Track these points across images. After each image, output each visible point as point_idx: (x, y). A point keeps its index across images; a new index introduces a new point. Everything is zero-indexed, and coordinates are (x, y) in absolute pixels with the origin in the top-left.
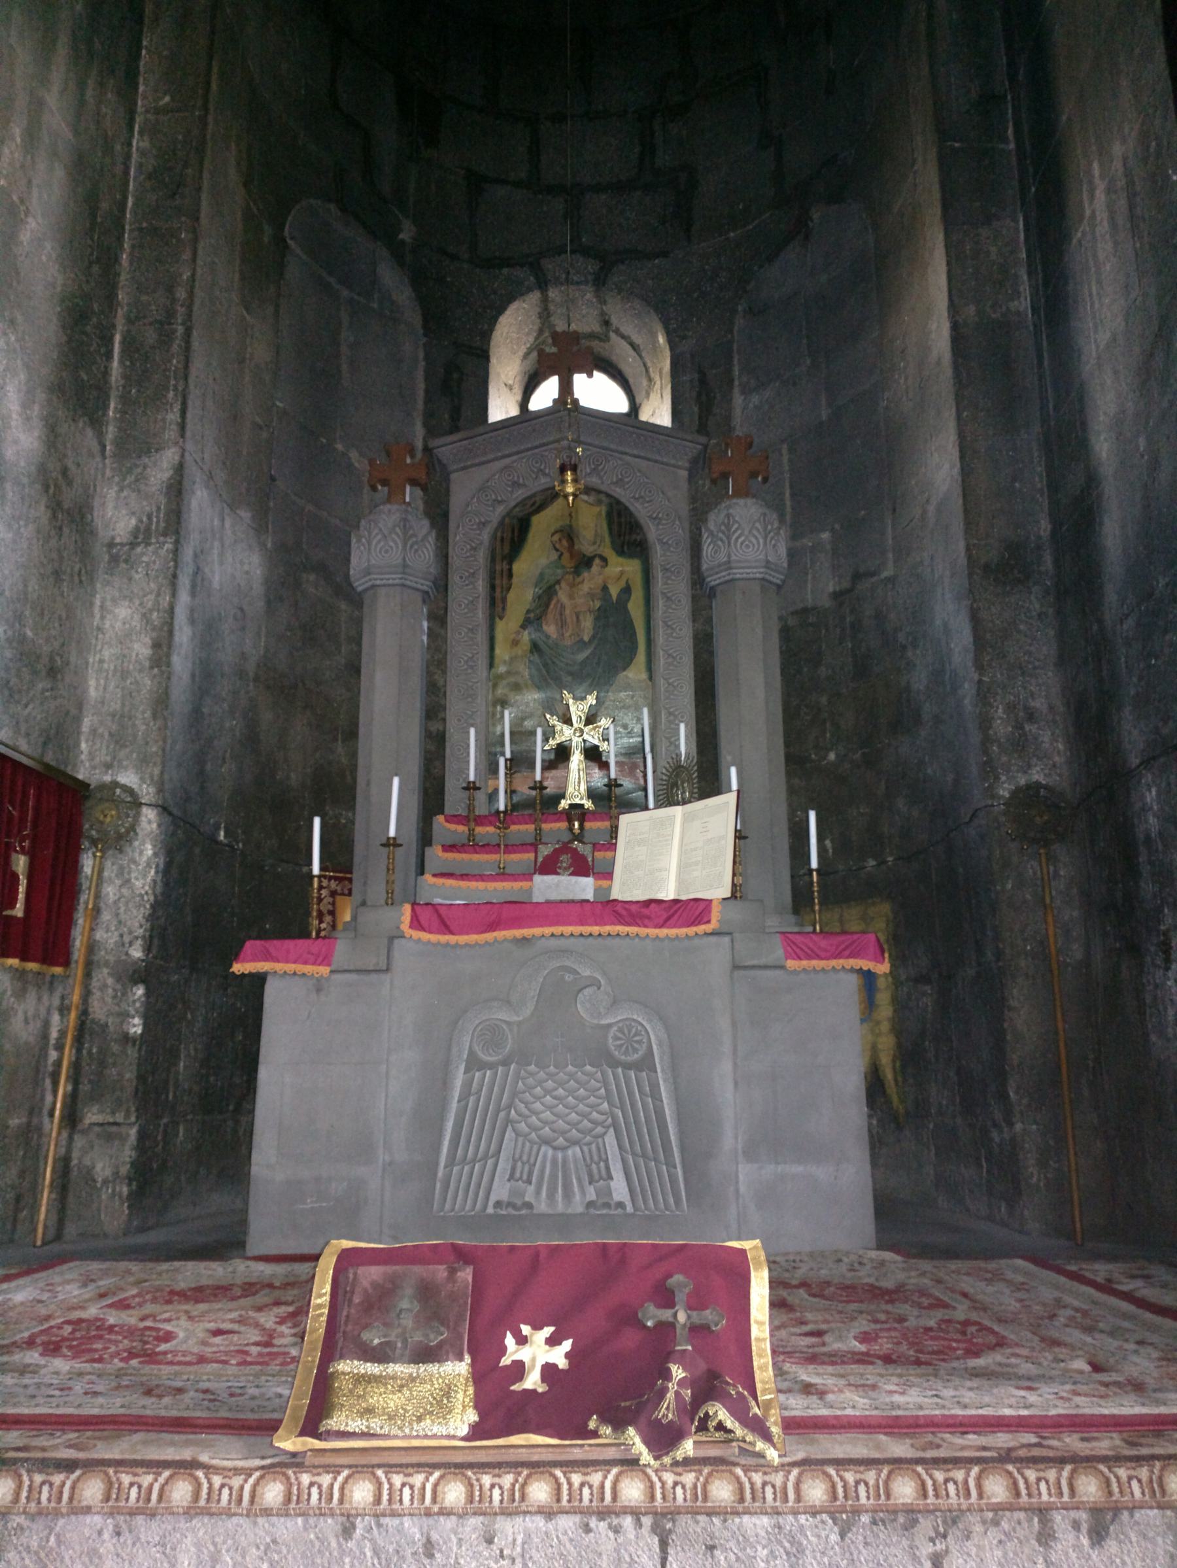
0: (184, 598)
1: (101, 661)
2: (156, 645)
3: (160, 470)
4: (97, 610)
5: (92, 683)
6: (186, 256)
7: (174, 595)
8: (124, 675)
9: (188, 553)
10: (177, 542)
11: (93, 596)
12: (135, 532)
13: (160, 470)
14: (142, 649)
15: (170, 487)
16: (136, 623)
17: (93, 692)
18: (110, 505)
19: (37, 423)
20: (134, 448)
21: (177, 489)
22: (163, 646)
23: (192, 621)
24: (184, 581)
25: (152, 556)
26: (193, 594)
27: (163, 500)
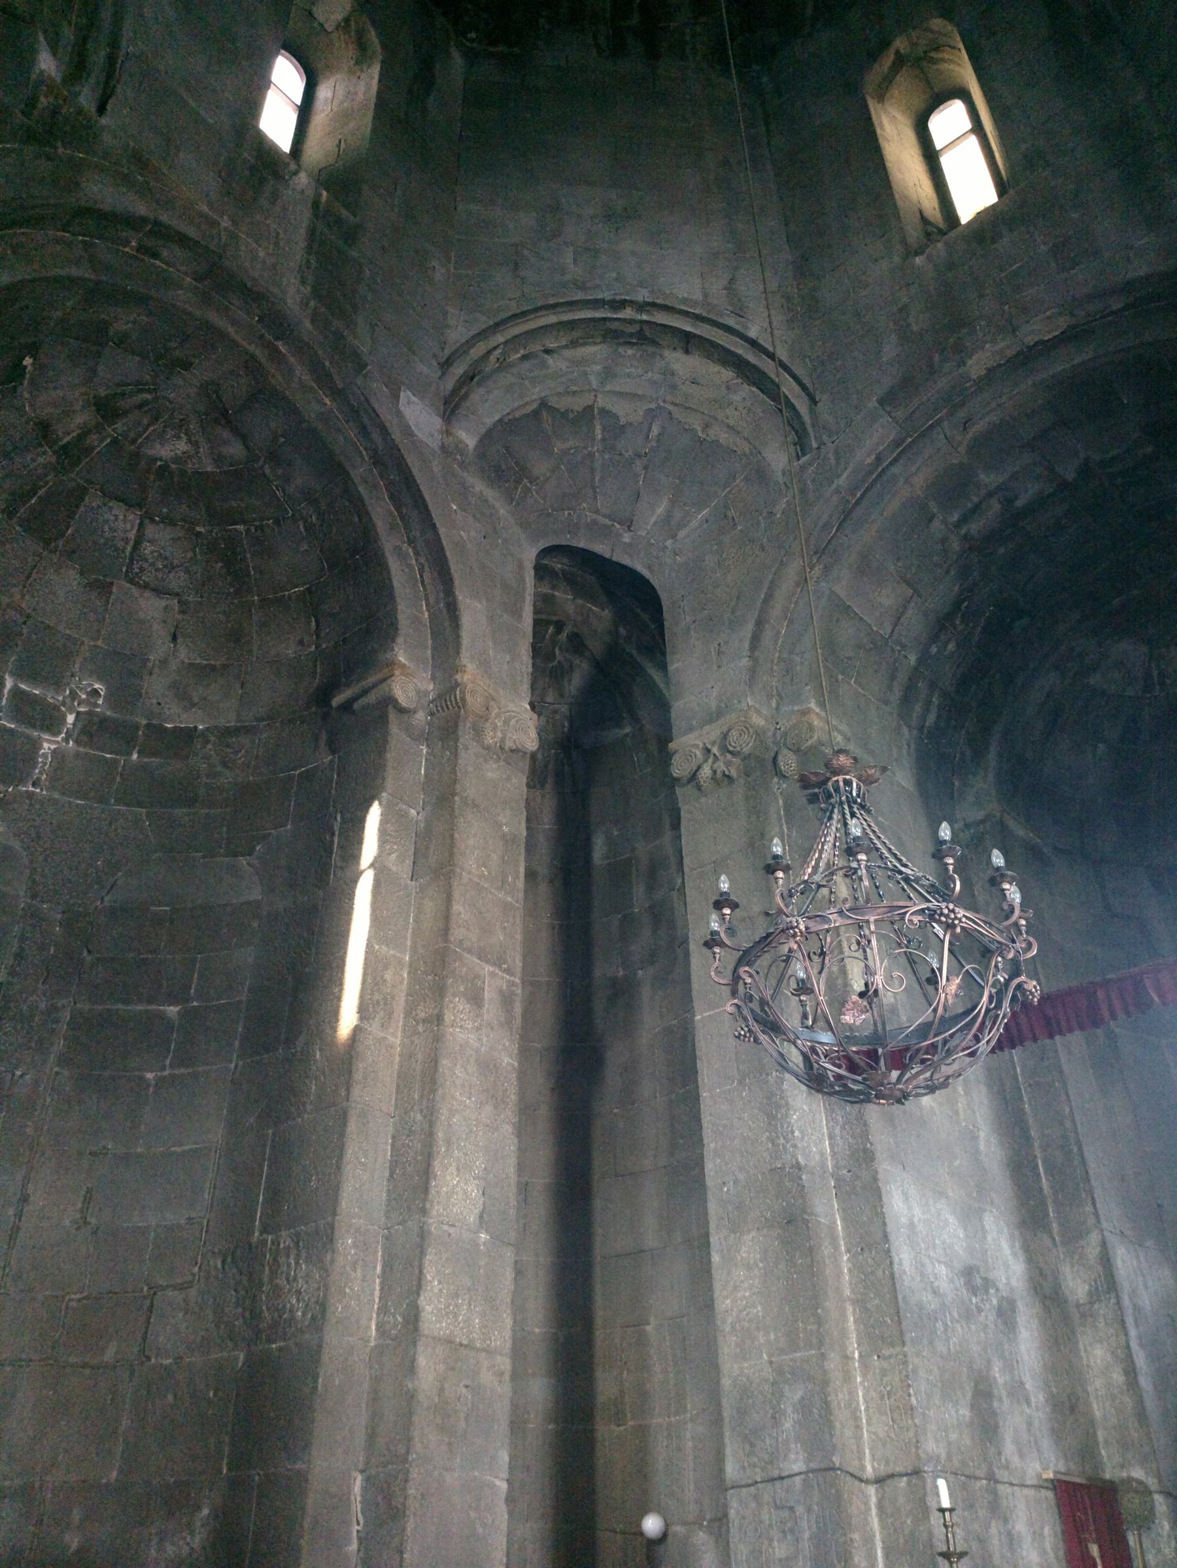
0: (1133, 1332)
1: (1096, 1390)
2: (1126, 1373)
3: (1091, 1246)
4: (1083, 1354)
5: (1095, 1406)
6: (1063, 1097)
7: (1126, 1335)
8: (1113, 1398)
9: (1126, 1301)
10: (1117, 1297)
11: (1077, 1342)
12: (1090, 1294)
13: (1092, 1251)
14: (1118, 1377)
15: (1101, 1259)
16: (1109, 1358)
17: (1098, 1414)
18: (1069, 1278)
19: (1020, 1252)
20: (1073, 1236)
21: (1106, 1260)
22: (1131, 1372)
23: (1141, 1346)
24: (1130, 1320)
25: (1103, 1309)
26: (1137, 1326)
27: (1100, 1269)
